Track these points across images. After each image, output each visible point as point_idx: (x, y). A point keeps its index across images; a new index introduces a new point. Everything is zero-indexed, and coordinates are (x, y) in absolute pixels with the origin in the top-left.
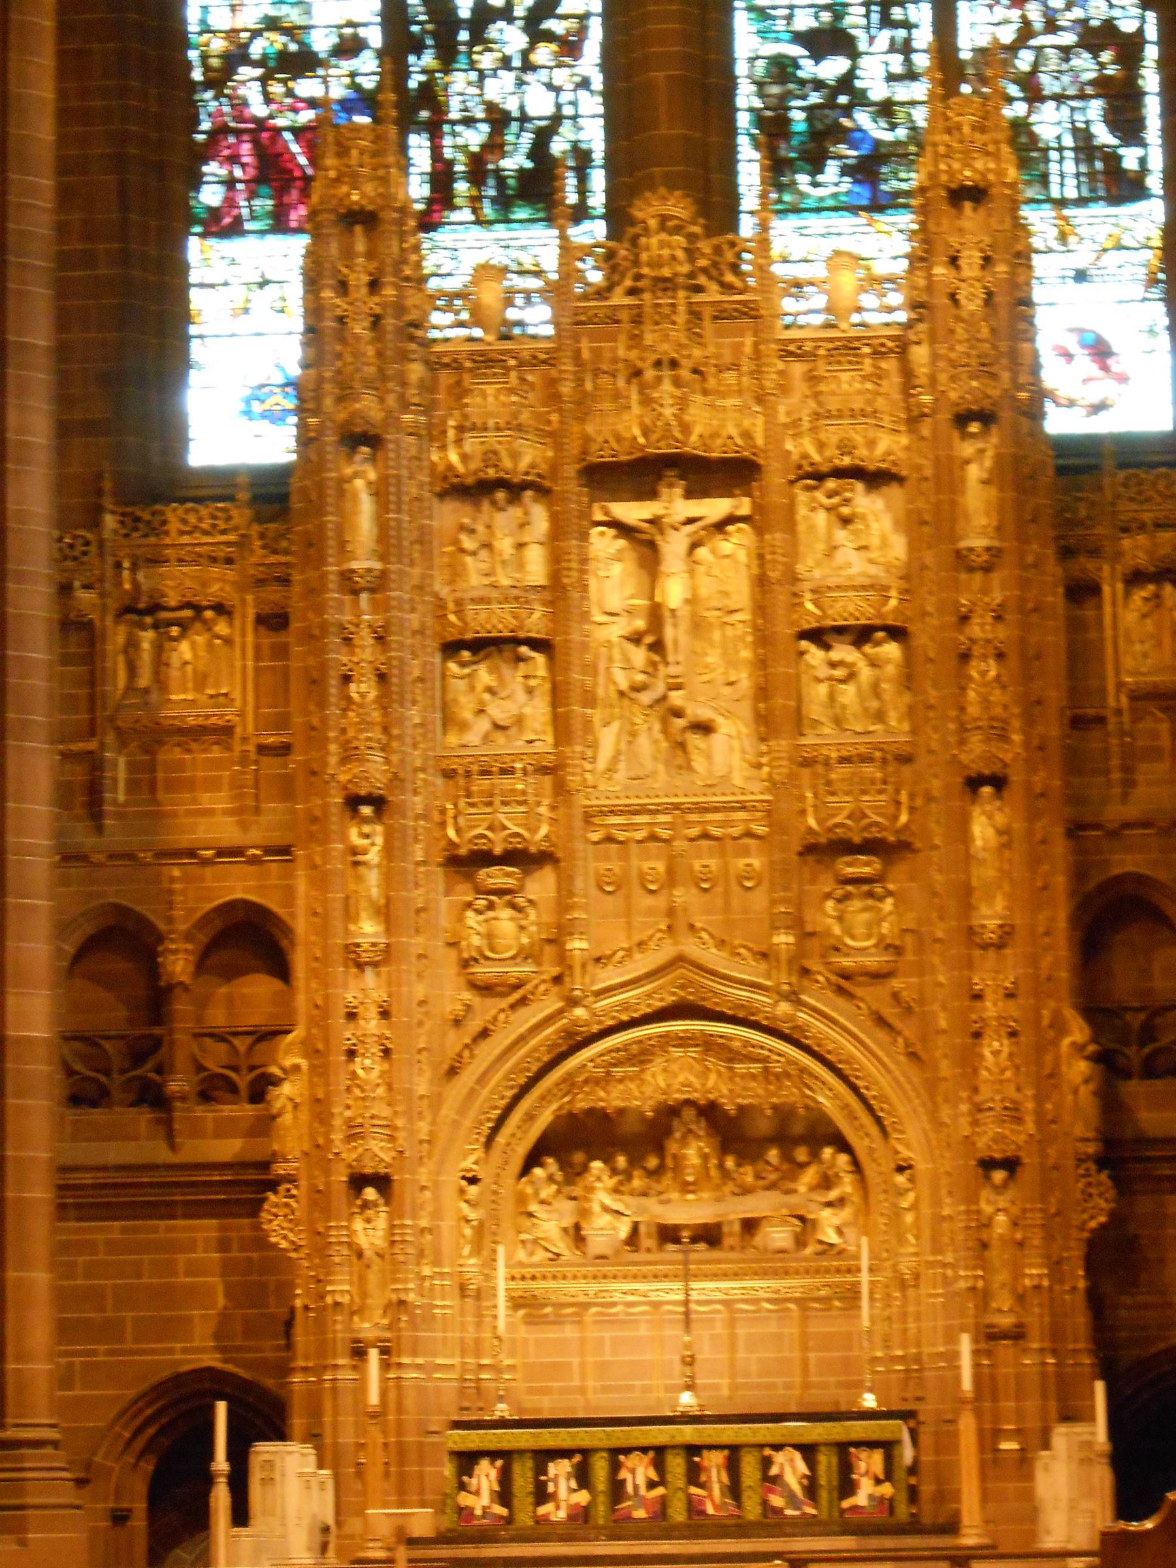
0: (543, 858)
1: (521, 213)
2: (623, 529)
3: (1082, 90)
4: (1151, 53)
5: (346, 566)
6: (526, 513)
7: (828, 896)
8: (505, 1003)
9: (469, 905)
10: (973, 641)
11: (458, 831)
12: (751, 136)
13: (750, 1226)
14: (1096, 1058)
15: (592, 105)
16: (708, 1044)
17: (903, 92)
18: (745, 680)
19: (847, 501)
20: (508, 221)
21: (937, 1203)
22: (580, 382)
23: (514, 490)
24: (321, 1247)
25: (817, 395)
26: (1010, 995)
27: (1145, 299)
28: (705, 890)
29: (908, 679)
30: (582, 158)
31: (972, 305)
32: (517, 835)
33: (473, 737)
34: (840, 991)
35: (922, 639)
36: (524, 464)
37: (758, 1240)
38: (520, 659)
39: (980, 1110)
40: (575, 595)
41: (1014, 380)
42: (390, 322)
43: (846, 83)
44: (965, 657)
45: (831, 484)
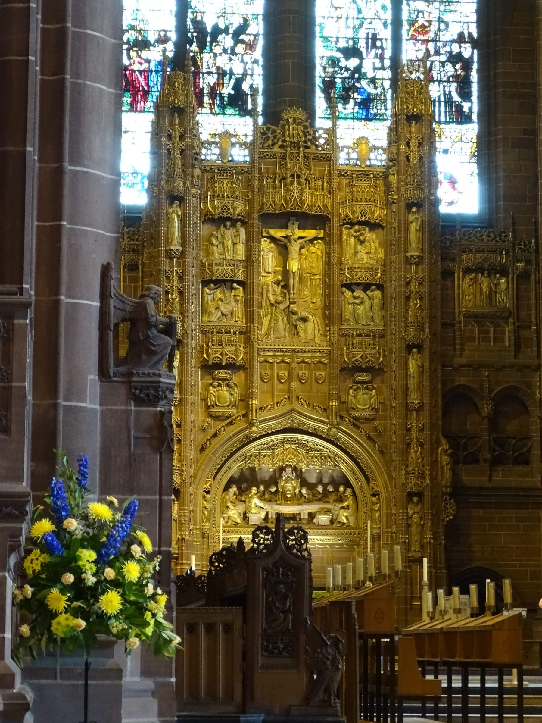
0: (242, 367)
1: (230, 111)
2: (273, 239)
3: (448, 78)
4: (475, 66)
5: (168, 248)
6: (237, 231)
7: (351, 388)
8: (224, 424)
9: (211, 384)
10: (412, 292)
11: (208, 355)
12: (320, 87)
14: (450, 455)
15: (259, 71)
16: (299, 443)
17: (380, 74)
18: (319, 302)
19: (362, 234)
20: (224, 114)
21: (389, 508)
22: (261, 181)
23: (234, 222)
25: (352, 192)
26: (421, 430)
27: (469, 162)
28: (303, 383)
29: (383, 306)
30: (254, 91)
31: (414, 161)
32: (232, 358)
33: (214, 319)
34: (354, 425)
35: (389, 290)
36: (237, 212)
37: (315, 521)
38: (232, 288)
39: (409, 474)
40: (256, 264)
41: (430, 191)
42: (188, 152)
43: (358, 69)
44: (408, 298)
45: (357, 227)
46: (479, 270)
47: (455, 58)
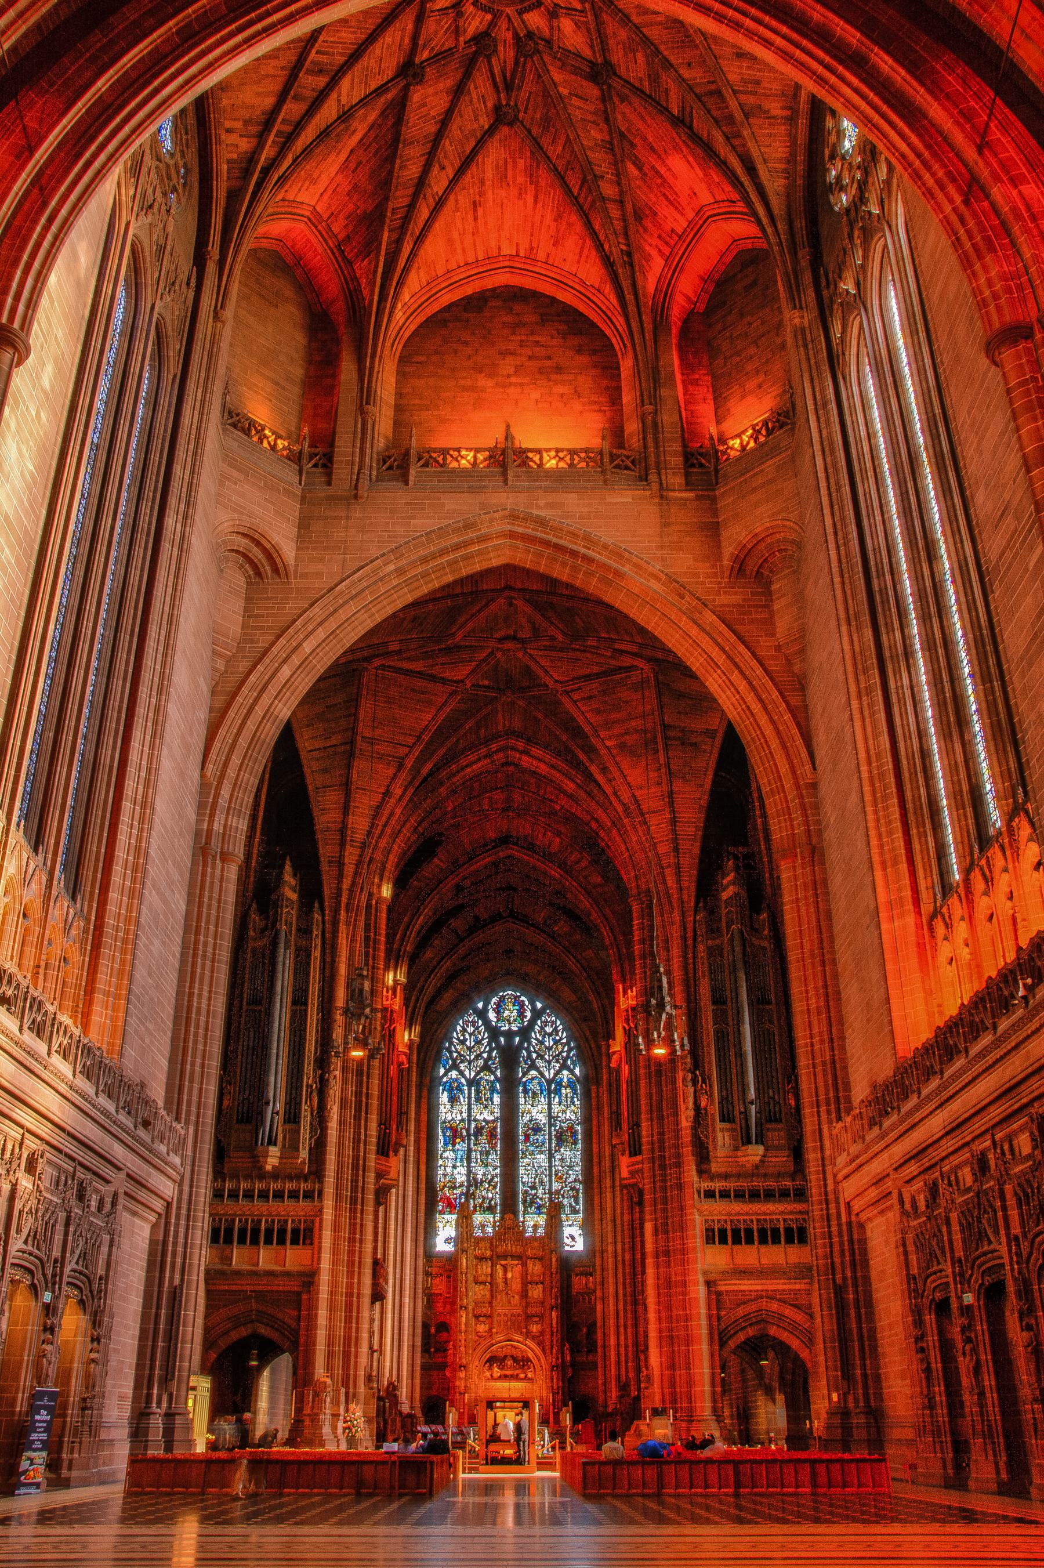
24: (454, 1377)
46: (581, 1274)
47: (573, 1189)
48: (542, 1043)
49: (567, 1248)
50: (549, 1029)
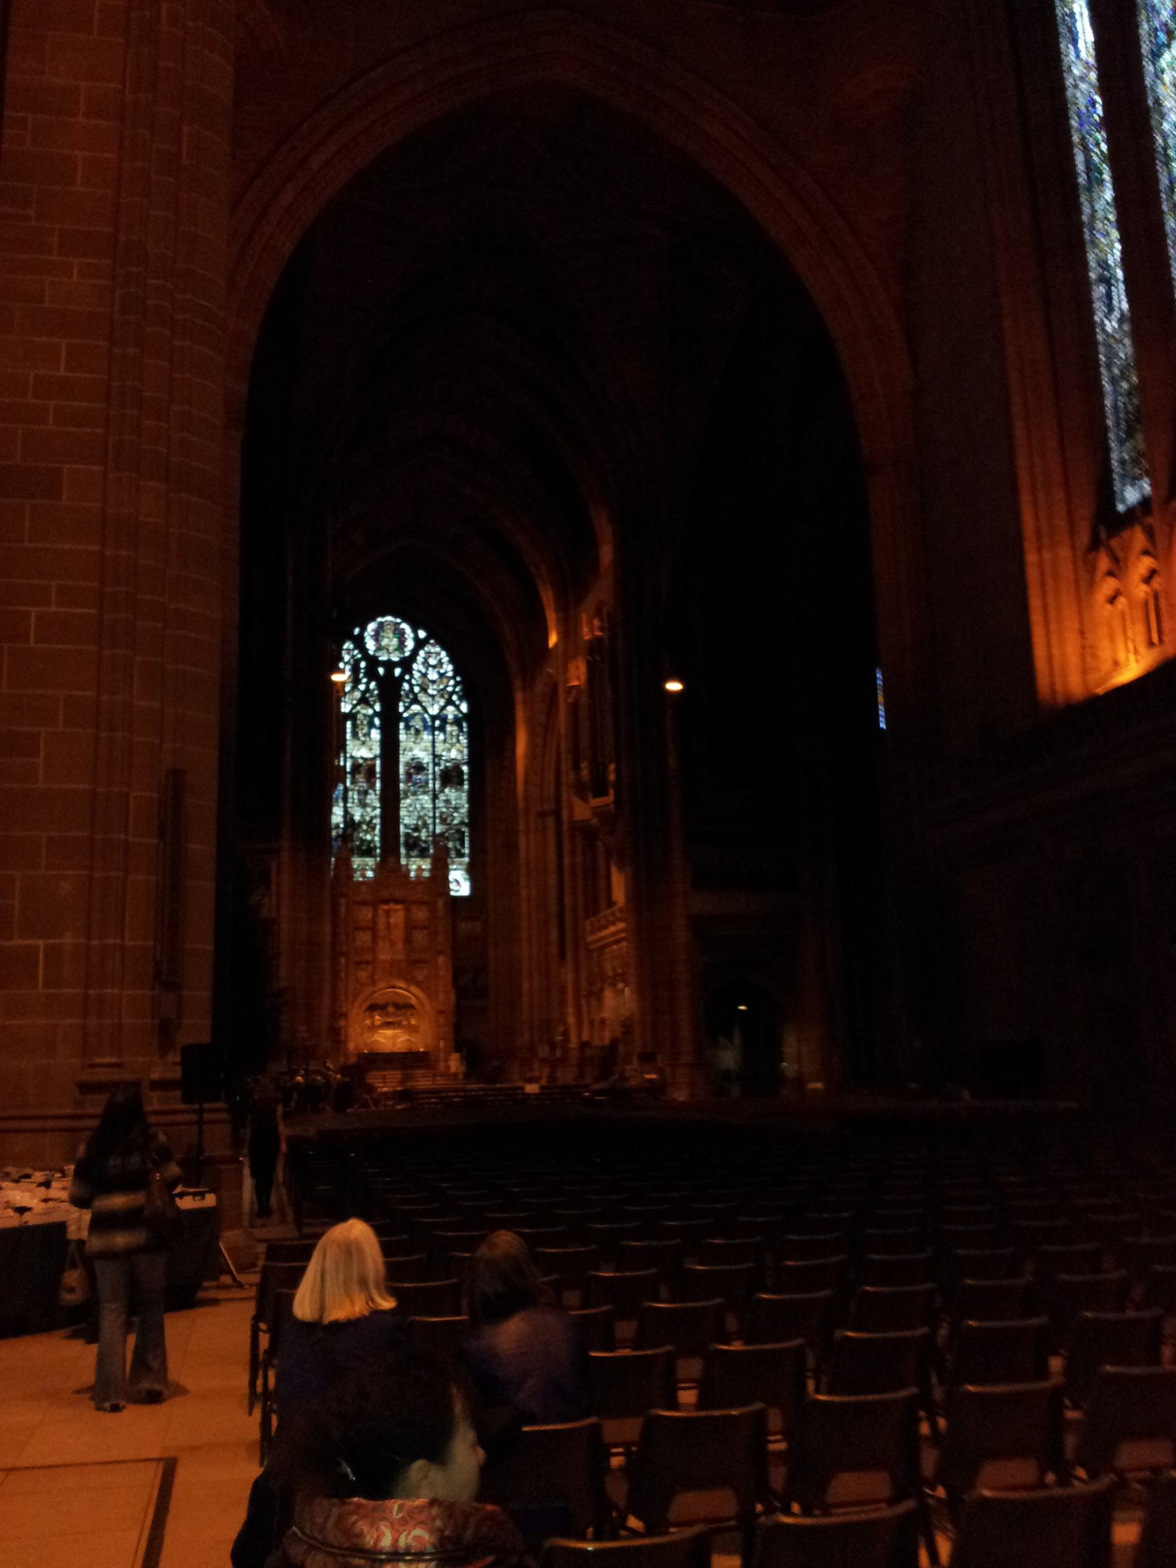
13: (400, 1021)
15: (377, 839)
30: (375, 848)
48: (424, 675)
49: (452, 893)
50: (432, 661)
